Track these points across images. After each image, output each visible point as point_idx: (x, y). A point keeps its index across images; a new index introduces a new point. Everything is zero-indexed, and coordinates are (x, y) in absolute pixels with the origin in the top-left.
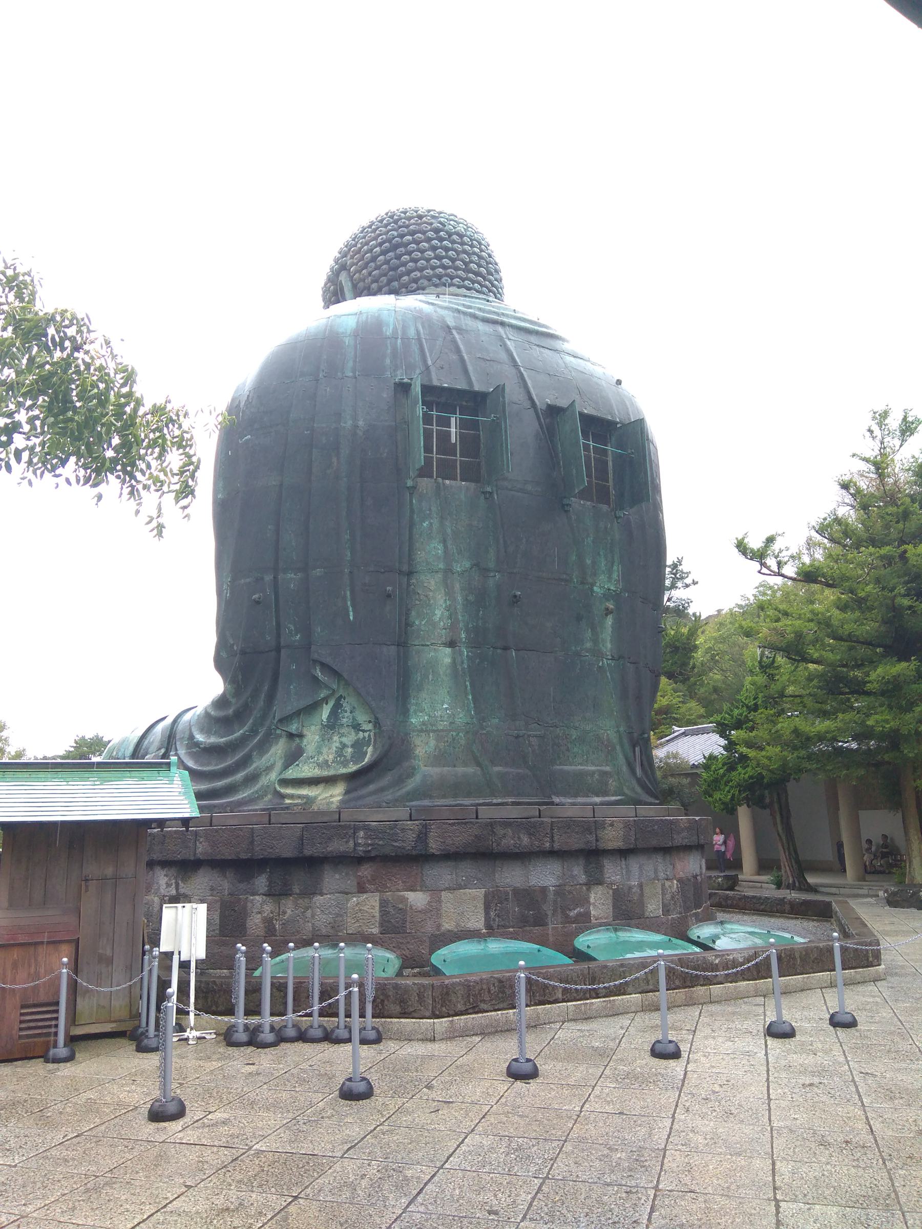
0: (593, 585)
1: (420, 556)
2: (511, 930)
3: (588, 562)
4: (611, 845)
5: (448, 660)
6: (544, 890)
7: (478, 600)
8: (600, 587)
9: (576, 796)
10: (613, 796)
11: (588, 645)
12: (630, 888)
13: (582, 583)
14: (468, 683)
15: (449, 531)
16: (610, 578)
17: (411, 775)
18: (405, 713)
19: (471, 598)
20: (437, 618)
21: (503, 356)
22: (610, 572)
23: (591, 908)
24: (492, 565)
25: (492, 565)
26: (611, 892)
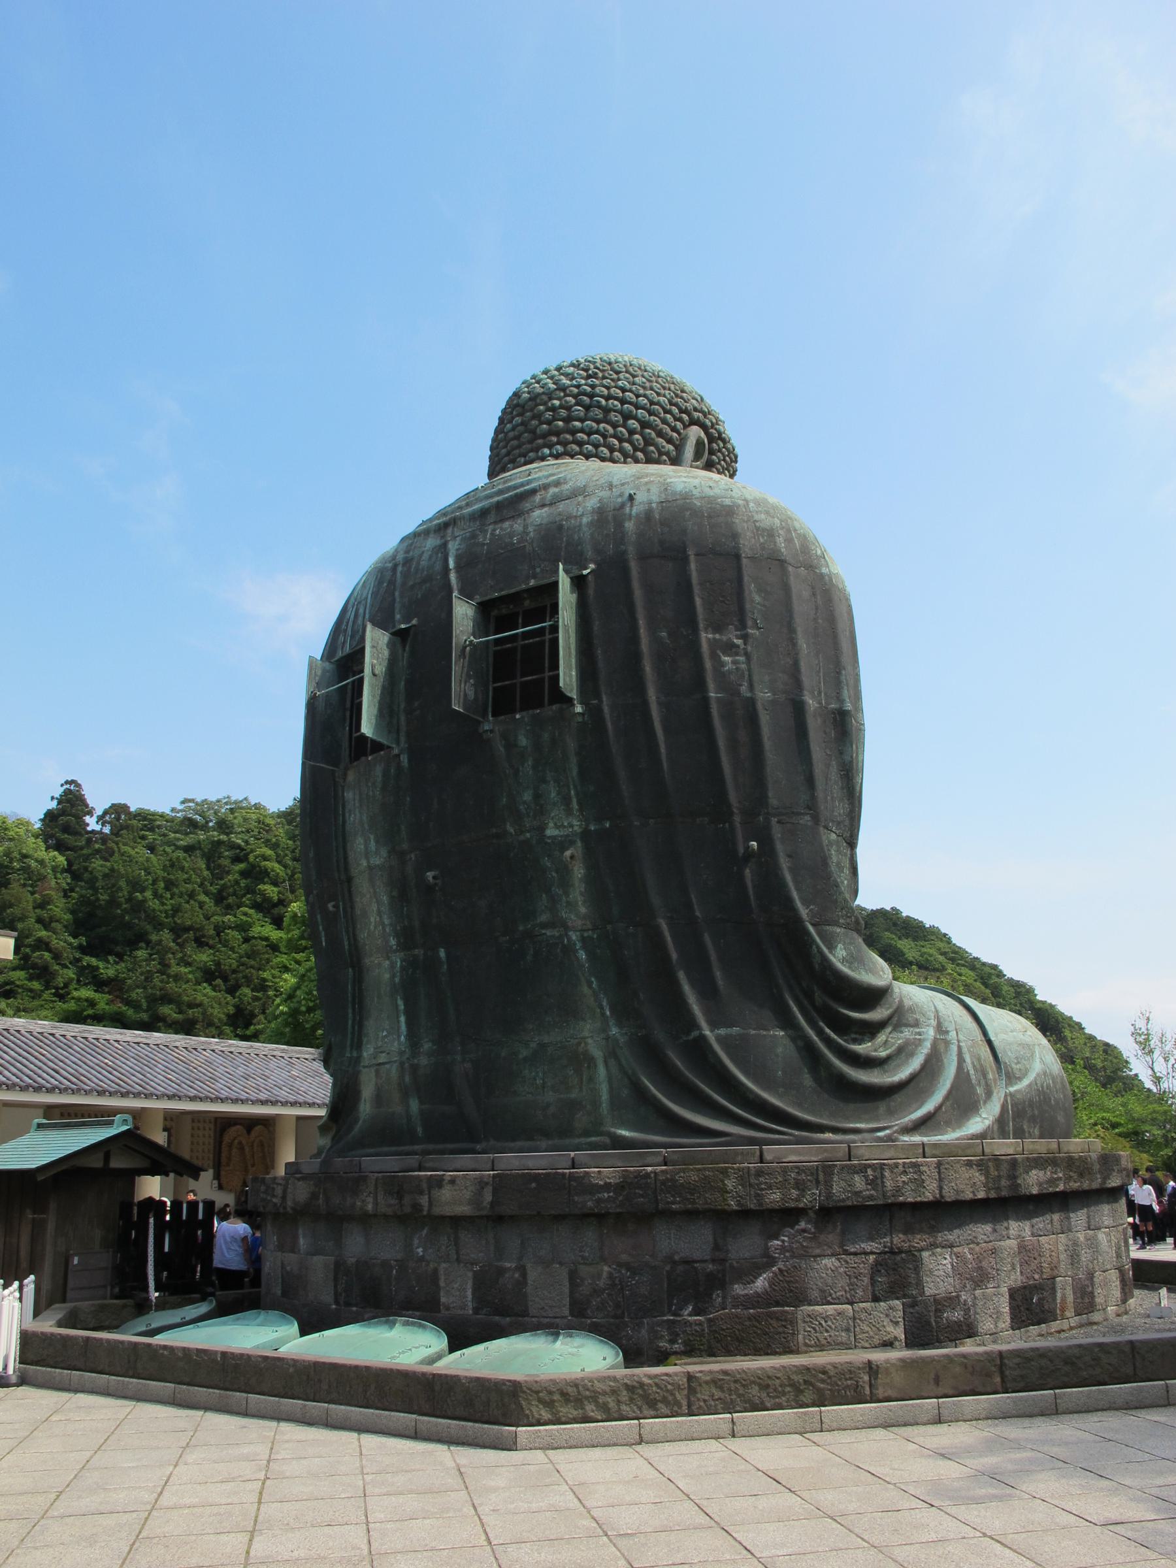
0: (542, 829)
1: (351, 855)
2: (354, 1309)
3: (527, 796)
4: (447, 1211)
5: (387, 976)
6: (385, 1264)
7: (402, 891)
8: (557, 827)
9: (514, 1140)
10: (580, 1136)
11: (544, 918)
12: (501, 1271)
13: (522, 832)
14: (400, 1003)
15: (364, 818)
16: (569, 812)
17: (356, 1120)
18: (358, 1046)
19: (395, 893)
20: (372, 928)
21: (438, 567)
22: (567, 801)
23: (442, 1294)
24: (405, 846)
25: (405, 846)
26: (470, 1274)
